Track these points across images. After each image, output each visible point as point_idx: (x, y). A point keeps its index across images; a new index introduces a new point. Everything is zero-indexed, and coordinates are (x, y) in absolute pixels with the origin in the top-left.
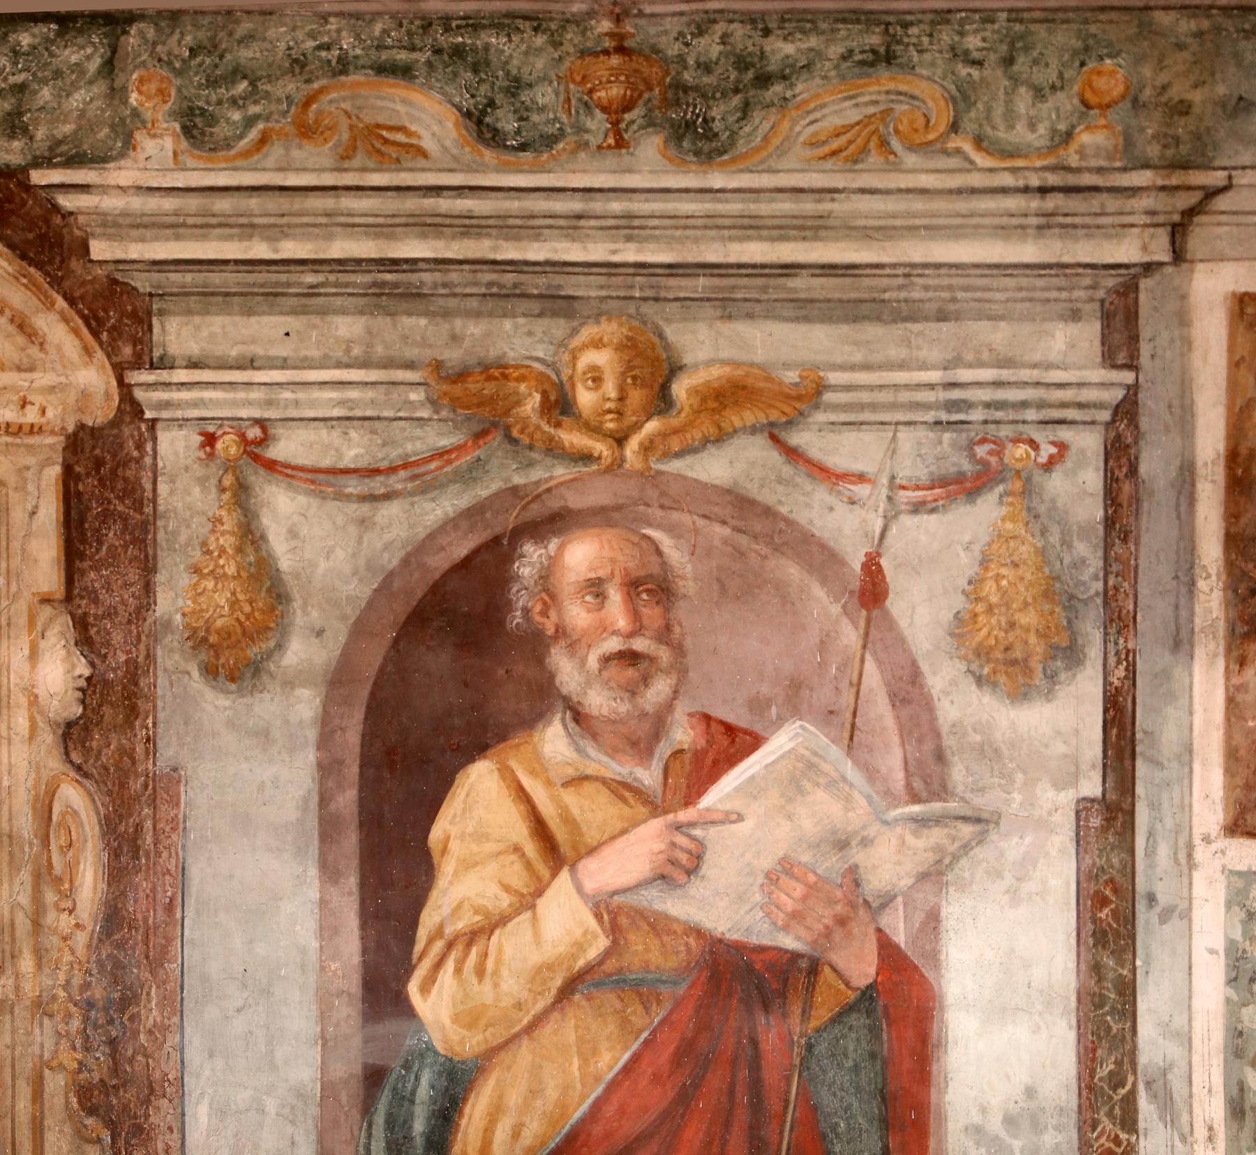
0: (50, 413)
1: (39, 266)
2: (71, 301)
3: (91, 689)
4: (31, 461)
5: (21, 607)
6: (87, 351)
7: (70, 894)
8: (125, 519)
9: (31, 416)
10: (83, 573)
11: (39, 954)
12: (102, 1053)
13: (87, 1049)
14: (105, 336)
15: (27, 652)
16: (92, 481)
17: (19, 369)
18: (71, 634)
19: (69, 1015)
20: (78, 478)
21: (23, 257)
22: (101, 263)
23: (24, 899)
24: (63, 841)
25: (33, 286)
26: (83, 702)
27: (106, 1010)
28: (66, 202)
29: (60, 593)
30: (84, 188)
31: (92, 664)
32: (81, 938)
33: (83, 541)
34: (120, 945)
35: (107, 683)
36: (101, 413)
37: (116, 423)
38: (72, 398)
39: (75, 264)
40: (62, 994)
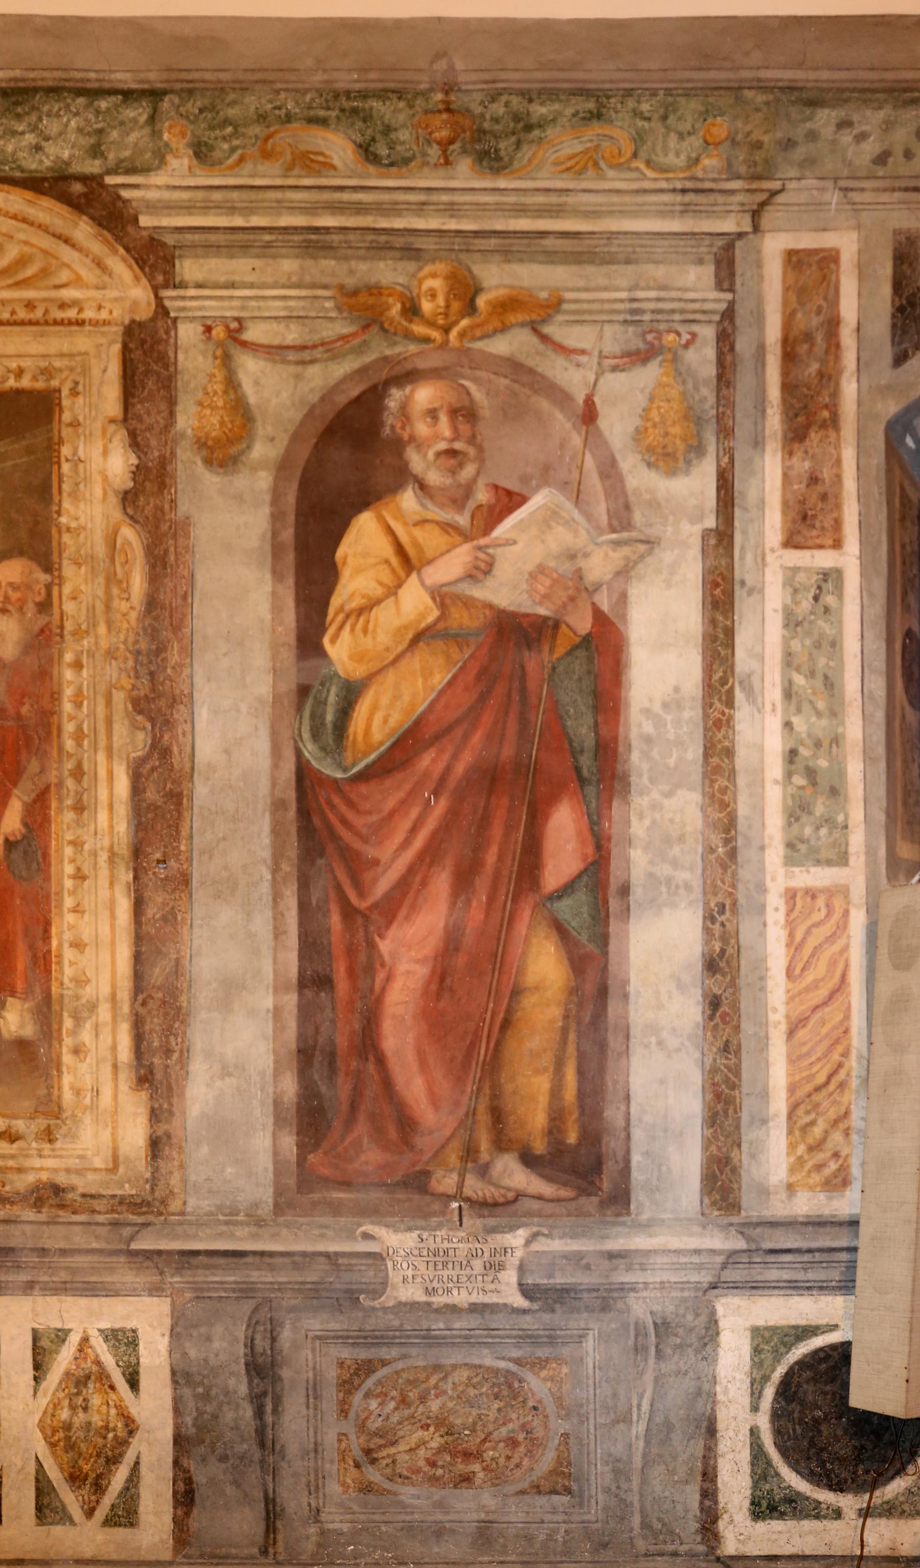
0: (115, 313)
3: (139, 472)
4: (104, 341)
5: (98, 425)
9: (104, 315)
11: (109, 624)
12: (145, 681)
13: (137, 677)
17: (97, 288)
18: (127, 440)
23: (100, 593)
24: (123, 560)
25: (106, 242)
32: (133, 615)
34: (156, 619)
35: (148, 469)
40: (122, 646)
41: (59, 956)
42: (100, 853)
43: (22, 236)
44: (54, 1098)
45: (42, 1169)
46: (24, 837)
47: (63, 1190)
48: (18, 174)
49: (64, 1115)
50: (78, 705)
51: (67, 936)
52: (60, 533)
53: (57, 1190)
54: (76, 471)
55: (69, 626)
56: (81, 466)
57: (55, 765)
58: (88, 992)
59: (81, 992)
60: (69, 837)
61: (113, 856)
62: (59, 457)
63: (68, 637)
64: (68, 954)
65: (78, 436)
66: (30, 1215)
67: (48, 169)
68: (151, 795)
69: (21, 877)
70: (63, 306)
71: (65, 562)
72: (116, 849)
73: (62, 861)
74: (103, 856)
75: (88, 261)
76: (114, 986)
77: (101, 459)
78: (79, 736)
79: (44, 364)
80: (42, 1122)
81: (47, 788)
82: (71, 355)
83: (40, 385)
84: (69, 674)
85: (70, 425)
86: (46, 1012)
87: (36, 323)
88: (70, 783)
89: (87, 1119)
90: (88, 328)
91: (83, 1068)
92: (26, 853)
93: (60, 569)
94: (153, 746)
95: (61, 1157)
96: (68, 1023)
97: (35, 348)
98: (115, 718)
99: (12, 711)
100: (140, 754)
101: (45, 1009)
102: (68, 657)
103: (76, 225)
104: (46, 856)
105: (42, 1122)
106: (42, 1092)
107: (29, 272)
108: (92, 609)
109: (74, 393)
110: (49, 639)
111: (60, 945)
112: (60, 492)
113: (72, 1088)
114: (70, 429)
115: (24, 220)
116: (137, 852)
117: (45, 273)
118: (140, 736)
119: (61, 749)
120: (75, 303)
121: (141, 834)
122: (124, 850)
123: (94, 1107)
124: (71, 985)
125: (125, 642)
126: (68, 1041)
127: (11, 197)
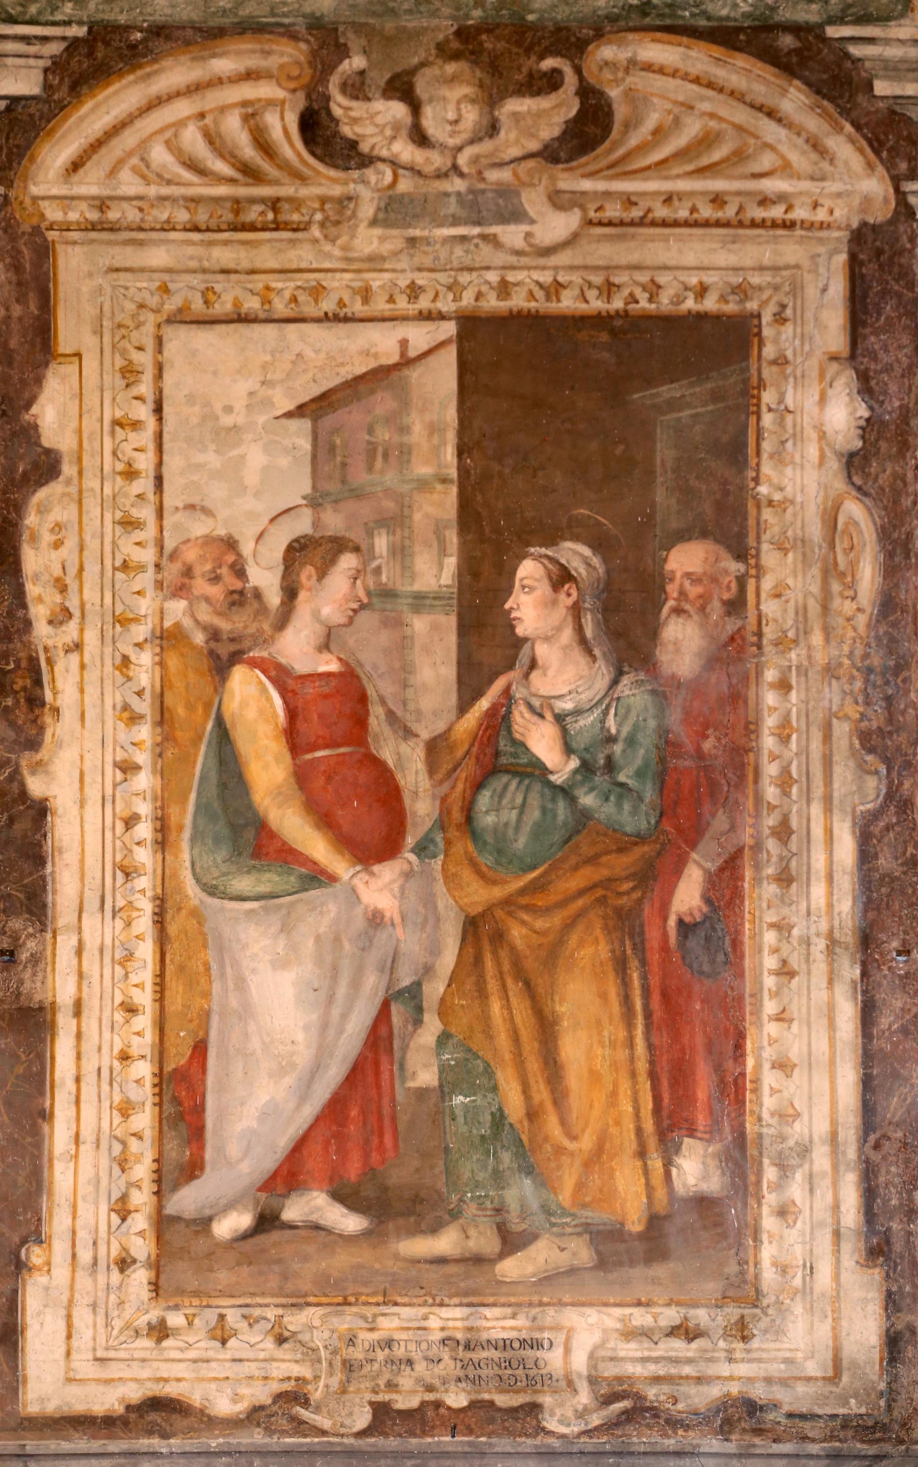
0: (837, 213)
1: (831, 100)
2: (858, 127)
3: (870, 428)
4: (822, 250)
5: (812, 366)
6: (870, 166)
7: (852, 586)
8: (899, 296)
9: (821, 215)
10: (865, 337)
11: (827, 631)
12: (879, 707)
13: (867, 703)
14: (884, 154)
15: (817, 397)
16: (873, 266)
17: (812, 178)
18: (855, 385)
19: (852, 678)
20: (862, 264)
21: (818, 92)
22: (883, 98)
23: (815, 588)
24: (846, 545)
25: (825, 115)
26: (863, 437)
27: (883, 674)
28: (855, 51)
29: (846, 353)
30: (871, 40)
31: (871, 408)
32: (862, 620)
33: (866, 312)
34: (894, 625)
35: (883, 423)
36: (880, 214)
37: (893, 221)
38: (856, 202)
39: (861, 98)
40: (847, 662)
41: (756, 1081)
42: (815, 940)
43: (706, 106)
44: (750, 1276)
45: (731, 1378)
46: (706, 918)
47: (761, 1408)
48: (703, 23)
49: (765, 1302)
50: (784, 740)
51: (768, 1053)
52: (758, 507)
53: (752, 1407)
54: (781, 423)
55: (769, 633)
56: (789, 418)
57: (751, 821)
58: (798, 1130)
59: (787, 1130)
60: (771, 917)
61: (832, 943)
62: (758, 406)
63: (768, 648)
64: (769, 1078)
65: (786, 378)
66: (713, 1444)
67: (744, 15)
68: (886, 862)
69: (702, 973)
70: (764, 201)
71: (765, 547)
72: (837, 935)
73: (760, 951)
74: (820, 945)
75: (800, 141)
76: (834, 1122)
77: (816, 410)
78: (785, 781)
79: (736, 280)
80: (733, 1312)
81: (740, 851)
82: (775, 269)
83: (731, 308)
84: (770, 698)
85: (774, 362)
86: (740, 1158)
87: (727, 224)
88: (772, 845)
89: (798, 1309)
90: (799, 232)
91: (792, 1235)
92: (708, 939)
93: (757, 556)
94: (890, 796)
95: (760, 1360)
96: (770, 1173)
97: (723, 258)
98: (836, 758)
99: (690, 747)
100: (870, 806)
101: (737, 1154)
102: (770, 675)
103: (784, 92)
104: (736, 943)
105: (733, 1312)
106: (732, 1268)
107: (717, 155)
108: (802, 612)
109: (780, 319)
110: (741, 650)
111: (758, 1067)
112: (758, 453)
113: (775, 1264)
114: (775, 369)
115: (710, 85)
116: (867, 940)
117: (739, 156)
118: (871, 782)
119: (758, 798)
120: (781, 198)
121: (871, 915)
122: (848, 935)
123: (806, 1291)
124: (774, 1121)
125: (850, 656)
126: (770, 1199)
127: (693, 53)
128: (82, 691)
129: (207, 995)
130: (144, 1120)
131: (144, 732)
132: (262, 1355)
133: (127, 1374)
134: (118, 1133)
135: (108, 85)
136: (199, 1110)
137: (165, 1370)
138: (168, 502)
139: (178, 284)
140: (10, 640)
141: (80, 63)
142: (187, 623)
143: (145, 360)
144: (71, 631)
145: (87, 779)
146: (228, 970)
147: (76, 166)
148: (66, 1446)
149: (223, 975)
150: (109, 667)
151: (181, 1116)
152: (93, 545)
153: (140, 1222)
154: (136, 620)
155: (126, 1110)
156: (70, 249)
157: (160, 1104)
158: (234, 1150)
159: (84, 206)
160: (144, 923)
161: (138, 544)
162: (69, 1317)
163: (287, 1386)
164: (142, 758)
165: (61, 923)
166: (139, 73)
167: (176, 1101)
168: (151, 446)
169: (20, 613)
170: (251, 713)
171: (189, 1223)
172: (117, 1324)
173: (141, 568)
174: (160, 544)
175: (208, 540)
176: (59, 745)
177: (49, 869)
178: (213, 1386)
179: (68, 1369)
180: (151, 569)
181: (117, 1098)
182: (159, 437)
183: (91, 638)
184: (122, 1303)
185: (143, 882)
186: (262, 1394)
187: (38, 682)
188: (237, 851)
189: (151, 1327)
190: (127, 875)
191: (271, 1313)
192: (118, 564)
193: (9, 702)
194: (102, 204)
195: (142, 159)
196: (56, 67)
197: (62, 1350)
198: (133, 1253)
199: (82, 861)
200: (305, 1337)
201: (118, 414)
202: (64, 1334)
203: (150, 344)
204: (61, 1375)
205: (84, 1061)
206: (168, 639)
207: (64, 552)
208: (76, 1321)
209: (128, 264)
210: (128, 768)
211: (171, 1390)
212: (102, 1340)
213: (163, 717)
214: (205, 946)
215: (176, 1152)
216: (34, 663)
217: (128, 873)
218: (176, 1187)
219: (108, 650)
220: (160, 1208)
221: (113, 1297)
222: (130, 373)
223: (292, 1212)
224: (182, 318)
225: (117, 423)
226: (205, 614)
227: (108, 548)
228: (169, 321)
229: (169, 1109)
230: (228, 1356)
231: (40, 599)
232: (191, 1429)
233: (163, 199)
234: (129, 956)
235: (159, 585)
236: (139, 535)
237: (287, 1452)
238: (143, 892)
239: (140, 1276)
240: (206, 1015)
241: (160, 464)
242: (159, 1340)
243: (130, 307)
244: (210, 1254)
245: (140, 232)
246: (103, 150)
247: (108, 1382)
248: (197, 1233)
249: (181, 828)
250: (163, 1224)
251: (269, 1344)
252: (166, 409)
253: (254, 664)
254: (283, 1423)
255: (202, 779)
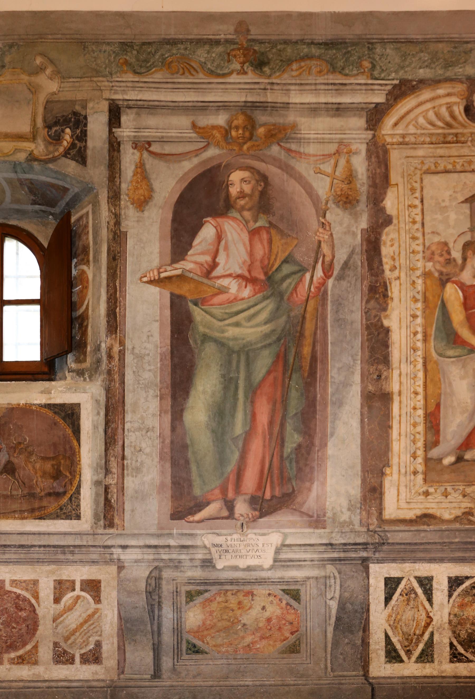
128: (400, 292)
129: (440, 388)
130: (421, 428)
131: (419, 305)
132: (458, 501)
133: (416, 507)
134: (413, 432)
135: (406, 98)
136: (438, 425)
137: (428, 505)
138: (426, 231)
139: (427, 161)
140: (378, 276)
141: (397, 92)
142: (433, 269)
143: (417, 186)
144: (396, 273)
145: (402, 320)
146: (446, 380)
147: (396, 124)
148: (397, 528)
149: (445, 382)
150: (409, 285)
151: (432, 427)
152: (403, 245)
153: (420, 460)
154: (417, 269)
155: (415, 425)
156: (394, 151)
157: (426, 423)
158: (449, 437)
159: (398, 137)
160: (420, 366)
161: (417, 245)
162: (398, 490)
163: (467, 510)
164: (419, 313)
165: (394, 366)
166: (415, 94)
167: (431, 422)
168: (420, 213)
169: (381, 268)
170: (453, 298)
171: (435, 460)
172: (413, 491)
173: (418, 252)
174: (424, 245)
175: (439, 243)
176: (393, 309)
177: (390, 349)
178: (443, 510)
179: (398, 505)
180: (421, 253)
181: (412, 422)
182: (423, 210)
183: (403, 275)
184: (414, 485)
185: (419, 353)
186: (459, 512)
187: (386, 290)
188: (448, 342)
189: (424, 493)
190: (414, 351)
191: (461, 488)
192: (411, 251)
193: (378, 296)
194: (403, 136)
195: (416, 122)
196: (390, 93)
197: (396, 500)
198: (418, 470)
199: (400, 346)
200: (472, 495)
201: (410, 203)
202: (397, 495)
203: (419, 180)
204: (396, 507)
205: (402, 410)
206: (427, 275)
207: (394, 248)
208: (400, 491)
209: (411, 155)
210: (414, 316)
211: (430, 511)
212: (408, 496)
213: (425, 300)
214: (439, 373)
215: (431, 438)
216: (385, 283)
217: (415, 350)
218: (431, 449)
219: (408, 279)
220: (426, 455)
221: (412, 484)
222: (413, 190)
223: (468, 456)
224: (428, 172)
225: (409, 206)
226: (438, 267)
227: (408, 246)
228: (425, 173)
229: (428, 425)
230: (448, 501)
231: (387, 263)
232: (437, 523)
233: (422, 134)
234: (416, 377)
235: (424, 258)
236: (417, 242)
237: (467, 530)
238: (419, 356)
239: (420, 477)
240: (440, 395)
241: (423, 219)
242: (426, 496)
243: (412, 169)
244: (442, 470)
245: (415, 145)
246: (404, 119)
247: (410, 509)
248: (438, 463)
249: (431, 335)
250: (427, 460)
251: (461, 497)
252: (425, 201)
253: (454, 282)
254: (466, 521)
255: (437, 319)
